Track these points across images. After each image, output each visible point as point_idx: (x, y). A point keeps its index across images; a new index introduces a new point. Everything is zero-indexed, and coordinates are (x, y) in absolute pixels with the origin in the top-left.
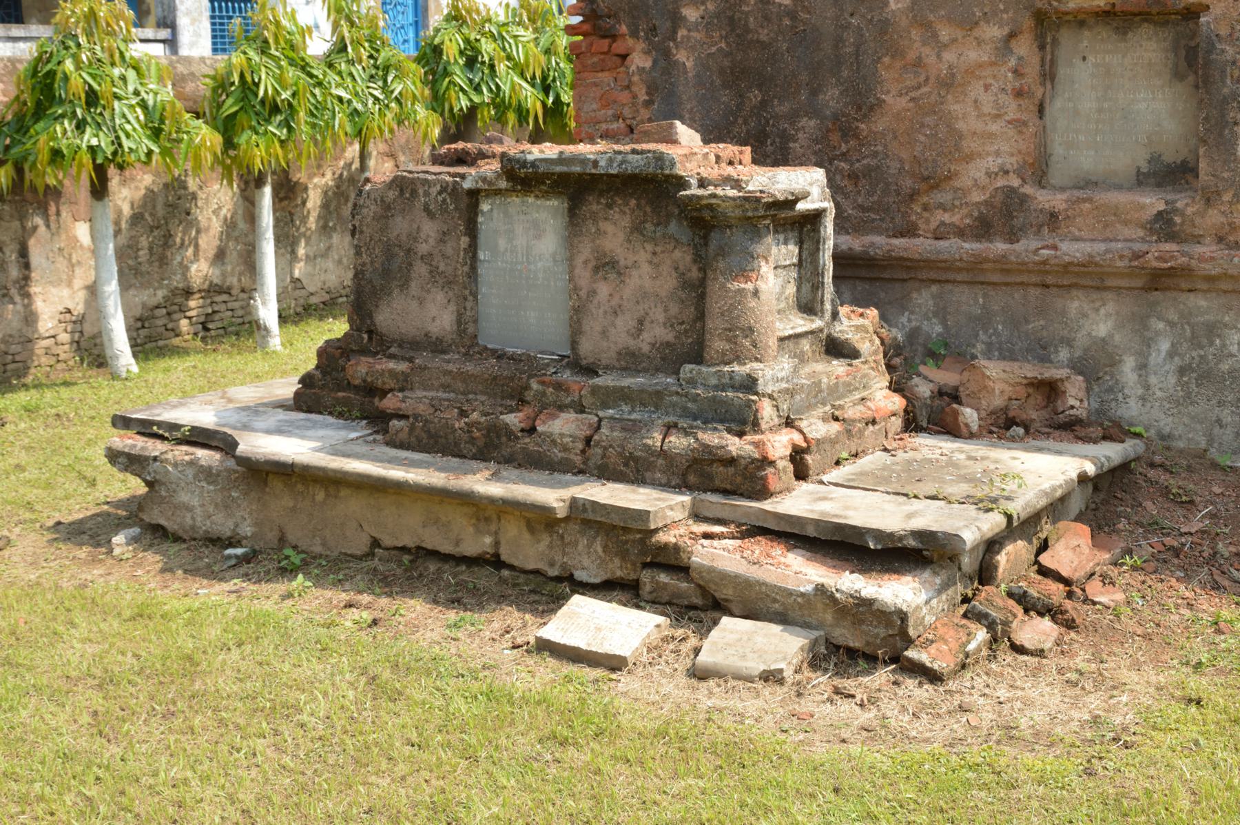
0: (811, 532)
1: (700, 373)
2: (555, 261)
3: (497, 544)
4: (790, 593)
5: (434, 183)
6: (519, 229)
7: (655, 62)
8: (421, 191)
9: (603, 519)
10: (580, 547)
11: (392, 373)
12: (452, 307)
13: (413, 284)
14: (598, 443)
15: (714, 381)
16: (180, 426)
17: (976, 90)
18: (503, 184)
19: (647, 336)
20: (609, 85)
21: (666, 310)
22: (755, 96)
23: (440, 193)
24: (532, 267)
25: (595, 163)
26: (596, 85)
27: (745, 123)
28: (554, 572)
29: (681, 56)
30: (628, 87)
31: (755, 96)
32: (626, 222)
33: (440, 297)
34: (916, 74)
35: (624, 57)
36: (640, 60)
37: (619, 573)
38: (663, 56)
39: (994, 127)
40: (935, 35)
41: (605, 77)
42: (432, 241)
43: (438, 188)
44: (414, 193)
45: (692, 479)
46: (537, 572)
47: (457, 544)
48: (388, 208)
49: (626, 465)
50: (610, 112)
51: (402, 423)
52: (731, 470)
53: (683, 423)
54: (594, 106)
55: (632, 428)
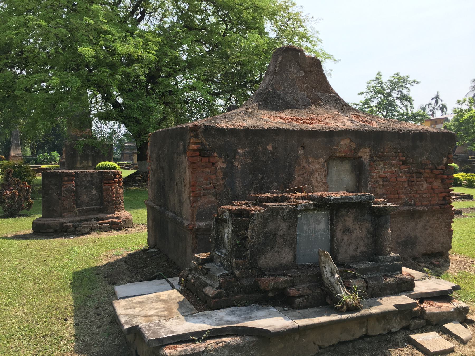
0: (435, 295)
1: (385, 258)
2: (324, 231)
3: (367, 330)
4: (449, 313)
5: (286, 209)
6: (312, 222)
7: (227, 166)
8: (281, 212)
9: (404, 309)
10: (393, 321)
11: (285, 281)
12: (292, 253)
13: (276, 247)
14: (370, 287)
15: (389, 260)
16: (206, 331)
17: (316, 175)
18: (312, 207)
19: (359, 251)
20: (208, 173)
21: (364, 242)
22: (260, 176)
23: (288, 212)
24: (316, 234)
25: (352, 199)
26: (203, 172)
27: (256, 184)
28: (385, 333)
29: (236, 164)
30: (215, 174)
31: (260, 176)
32: (352, 216)
33: (287, 250)
34: (303, 171)
35: (213, 164)
36: (221, 165)
37: (404, 325)
38: (230, 164)
39: (320, 184)
40: (309, 161)
41: (207, 170)
42: (284, 230)
43: (288, 210)
44: (278, 213)
45: (397, 290)
46: (379, 334)
47: (353, 336)
48: (267, 219)
49: (380, 291)
50: (208, 182)
51: (301, 299)
52: (406, 284)
53: (389, 274)
54: (202, 179)
55: (377, 279)
